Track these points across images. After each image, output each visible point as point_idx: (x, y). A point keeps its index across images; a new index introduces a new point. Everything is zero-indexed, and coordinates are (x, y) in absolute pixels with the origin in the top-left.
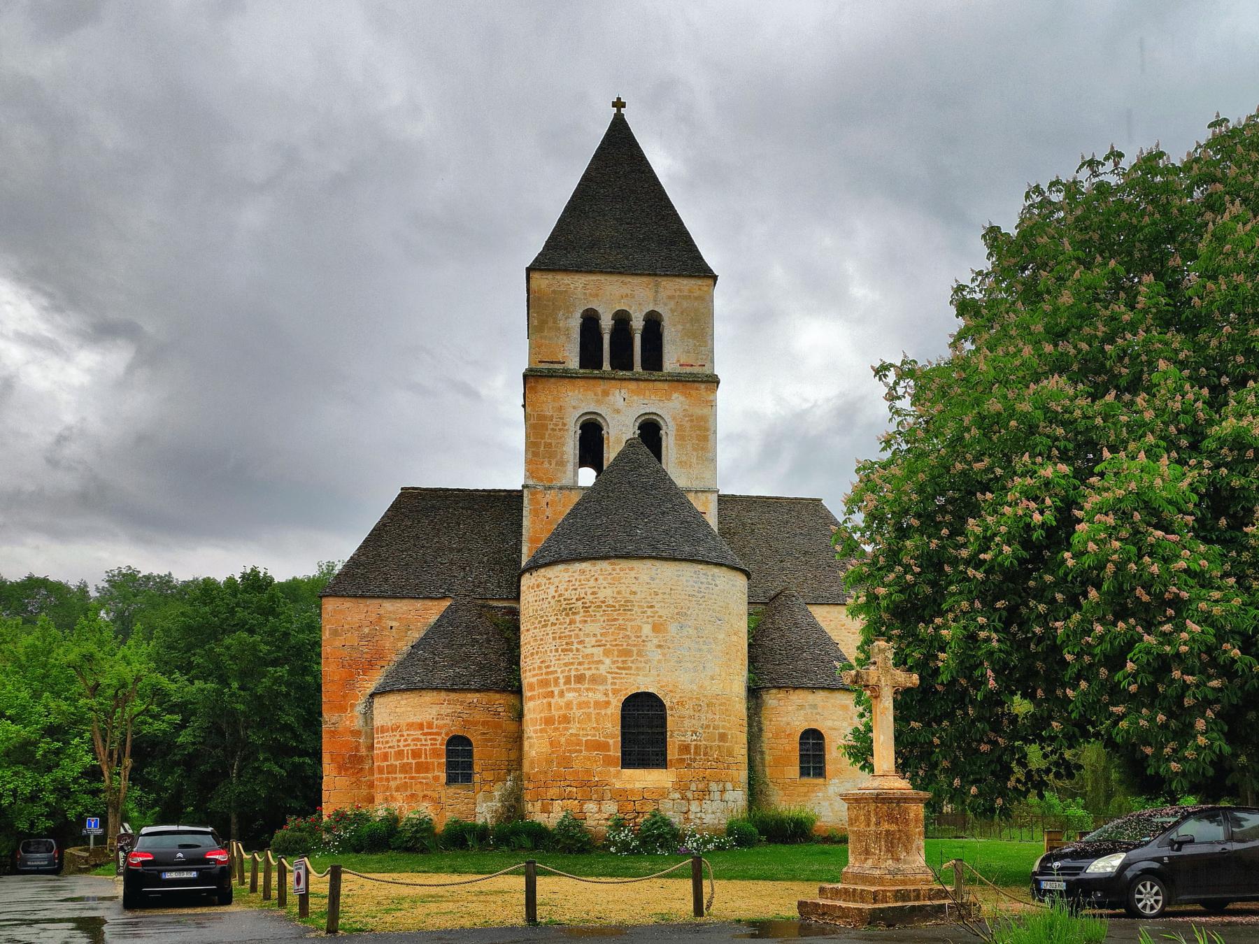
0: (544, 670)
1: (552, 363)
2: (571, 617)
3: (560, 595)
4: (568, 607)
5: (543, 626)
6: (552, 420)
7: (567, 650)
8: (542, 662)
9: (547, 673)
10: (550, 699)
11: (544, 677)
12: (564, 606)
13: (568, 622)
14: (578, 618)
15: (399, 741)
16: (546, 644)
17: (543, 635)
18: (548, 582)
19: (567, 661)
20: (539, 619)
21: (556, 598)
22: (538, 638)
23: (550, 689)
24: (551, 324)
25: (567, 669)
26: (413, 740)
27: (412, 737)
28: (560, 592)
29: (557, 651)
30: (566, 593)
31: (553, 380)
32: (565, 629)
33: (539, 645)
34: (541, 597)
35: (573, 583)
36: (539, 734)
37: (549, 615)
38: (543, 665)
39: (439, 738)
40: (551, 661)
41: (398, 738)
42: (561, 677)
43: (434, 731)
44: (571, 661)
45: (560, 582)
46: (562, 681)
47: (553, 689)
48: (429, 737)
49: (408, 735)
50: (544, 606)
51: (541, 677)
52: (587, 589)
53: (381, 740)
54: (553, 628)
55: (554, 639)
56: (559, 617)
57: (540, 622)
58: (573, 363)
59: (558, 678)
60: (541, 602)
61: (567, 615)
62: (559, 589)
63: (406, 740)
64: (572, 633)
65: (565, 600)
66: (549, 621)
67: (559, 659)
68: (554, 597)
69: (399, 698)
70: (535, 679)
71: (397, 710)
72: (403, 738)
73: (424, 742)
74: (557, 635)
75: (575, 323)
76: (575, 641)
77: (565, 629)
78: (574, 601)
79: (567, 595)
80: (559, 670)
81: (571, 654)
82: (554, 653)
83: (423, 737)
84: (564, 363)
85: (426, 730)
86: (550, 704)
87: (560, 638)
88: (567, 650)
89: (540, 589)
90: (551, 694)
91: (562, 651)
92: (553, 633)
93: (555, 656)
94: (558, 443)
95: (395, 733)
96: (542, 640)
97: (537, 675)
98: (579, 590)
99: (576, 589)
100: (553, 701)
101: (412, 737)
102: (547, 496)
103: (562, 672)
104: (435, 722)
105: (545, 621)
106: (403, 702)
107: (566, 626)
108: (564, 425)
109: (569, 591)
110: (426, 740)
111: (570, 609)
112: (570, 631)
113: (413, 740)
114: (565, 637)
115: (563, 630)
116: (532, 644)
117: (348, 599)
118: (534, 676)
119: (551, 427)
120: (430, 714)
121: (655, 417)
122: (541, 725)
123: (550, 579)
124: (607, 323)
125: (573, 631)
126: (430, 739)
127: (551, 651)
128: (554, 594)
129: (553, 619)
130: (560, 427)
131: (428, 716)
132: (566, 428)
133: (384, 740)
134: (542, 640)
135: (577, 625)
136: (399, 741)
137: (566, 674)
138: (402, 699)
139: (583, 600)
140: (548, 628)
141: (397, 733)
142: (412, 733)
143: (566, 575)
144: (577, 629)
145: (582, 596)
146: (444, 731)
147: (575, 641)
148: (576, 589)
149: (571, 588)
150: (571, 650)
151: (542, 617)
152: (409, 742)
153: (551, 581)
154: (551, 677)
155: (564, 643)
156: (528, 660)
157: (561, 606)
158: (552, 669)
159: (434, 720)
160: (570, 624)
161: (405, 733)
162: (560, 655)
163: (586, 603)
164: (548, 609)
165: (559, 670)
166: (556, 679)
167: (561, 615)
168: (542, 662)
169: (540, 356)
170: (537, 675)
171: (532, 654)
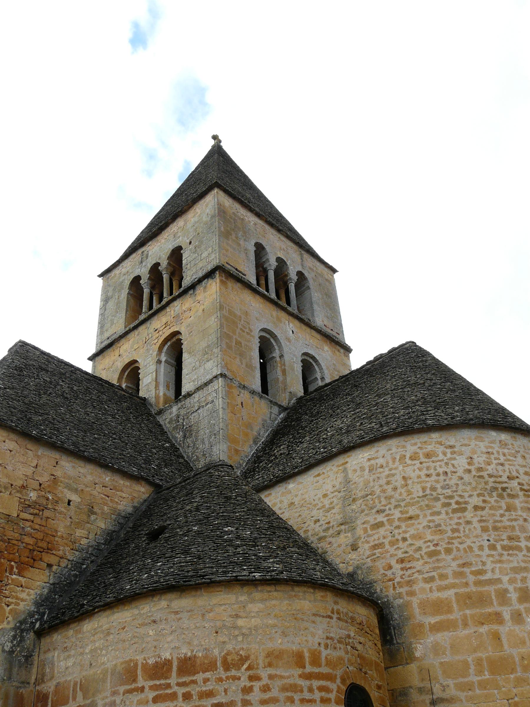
0: (471, 578)
1: (236, 269)
2: (508, 500)
3: (480, 469)
4: (499, 486)
5: (454, 511)
6: (240, 320)
7: (511, 548)
8: (464, 565)
9: (478, 583)
10: (495, 627)
11: (473, 588)
12: (491, 484)
13: (505, 507)
14: (517, 502)
15: (247, 690)
16: (467, 536)
17: (458, 524)
18: (449, 451)
19: (515, 564)
20: (443, 500)
21: (474, 473)
22: (449, 528)
23: (490, 610)
24: (233, 236)
25: (519, 577)
26: (284, 689)
27: (279, 683)
28: (477, 465)
29: (493, 547)
30: (489, 468)
31: (239, 285)
32: (502, 516)
33: (452, 538)
34: (441, 470)
35: (496, 455)
36: (478, 691)
37: (466, 495)
38: (467, 570)
39: (333, 686)
40: (484, 564)
41: (244, 682)
42: (511, 588)
43: (325, 670)
44: (523, 565)
45: (474, 452)
46: (514, 596)
47: (498, 609)
48: (316, 683)
49: (271, 677)
50: (452, 482)
51: (462, 590)
52: (518, 467)
53: (181, 691)
54: (479, 513)
55: (485, 529)
56: (487, 498)
57: (449, 504)
58: (253, 280)
59: (506, 591)
60: (442, 478)
61: (501, 496)
62: (475, 461)
63: (266, 689)
64: (515, 523)
65: (490, 476)
66: (466, 503)
67: (500, 562)
68: (469, 471)
69: (243, 598)
70: (451, 593)
71: (240, 622)
72: (257, 685)
73: (307, 695)
74: (490, 525)
75: (252, 249)
76: (522, 535)
77: (502, 516)
78: (504, 479)
79: (490, 469)
80: (505, 579)
81: (520, 555)
82: (487, 551)
83: (304, 683)
84: (245, 275)
85: (309, 669)
86: (497, 637)
87: (495, 529)
88: (511, 548)
89: (434, 459)
90: (498, 618)
91: (504, 548)
92: (480, 521)
93: (492, 556)
94: (246, 345)
95: (233, 672)
96: (454, 531)
97: (453, 586)
98: (507, 467)
99: (502, 465)
100: (504, 630)
101: (279, 683)
102: (242, 395)
103: (512, 581)
104: (324, 653)
105: (457, 503)
106: (255, 607)
107: (502, 512)
108: (251, 331)
109: (493, 466)
110: (311, 690)
111: (504, 489)
112: (512, 520)
113: (284, 689)
114: (505, 528)
115: (498, 518)
116: (429, 537)
117: (12, 436)
118: (441, 589)
119: (240, 326)
120: (313, 635)
121: (311, 361)
122: (480, 672)
123: (451, 447)
124: (272, 264)
125: (516, 520)
126: (321, 689)
127: (481, 548)
128: (467, 467)
129: (476, 501)
130: (247, 330)
131: (310, 638)
132: (252, 334)
133: (194, 690)
134: (457, 530)
135: (520, 513)
136: (247, 690)
137: (519, 585)
138: (253, 601)
139: (517, 480)
140: (469, 515)
141: (243, 673)
142: (278, 673)
143: (481, 444)
144: (521, 519)
145: (515, 474)
146: (339, 673)
147: (522, 535)
148: (502, 465)
149: (495, 462)
150: (519, 549)
151: (451, 497)
152: (274, 693)
153: (456, 450)
154: (491, 589)
155: (504, 537)
156: (418, 565)
157: (486, 483)
158: (488, 576)
159: (322, 648)
160: (509, 509)
161: (264, 674)
162: (501, 555)
163: (523, 485)
164: (461, 487)
165: (505, 579)
166: (503, 595)
167: (491, 496)
168: (464, 565)
169: (227, 259)
170: (453, 586)
171: (431, 554)
